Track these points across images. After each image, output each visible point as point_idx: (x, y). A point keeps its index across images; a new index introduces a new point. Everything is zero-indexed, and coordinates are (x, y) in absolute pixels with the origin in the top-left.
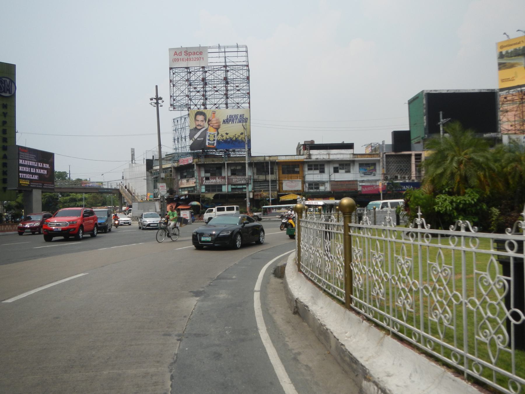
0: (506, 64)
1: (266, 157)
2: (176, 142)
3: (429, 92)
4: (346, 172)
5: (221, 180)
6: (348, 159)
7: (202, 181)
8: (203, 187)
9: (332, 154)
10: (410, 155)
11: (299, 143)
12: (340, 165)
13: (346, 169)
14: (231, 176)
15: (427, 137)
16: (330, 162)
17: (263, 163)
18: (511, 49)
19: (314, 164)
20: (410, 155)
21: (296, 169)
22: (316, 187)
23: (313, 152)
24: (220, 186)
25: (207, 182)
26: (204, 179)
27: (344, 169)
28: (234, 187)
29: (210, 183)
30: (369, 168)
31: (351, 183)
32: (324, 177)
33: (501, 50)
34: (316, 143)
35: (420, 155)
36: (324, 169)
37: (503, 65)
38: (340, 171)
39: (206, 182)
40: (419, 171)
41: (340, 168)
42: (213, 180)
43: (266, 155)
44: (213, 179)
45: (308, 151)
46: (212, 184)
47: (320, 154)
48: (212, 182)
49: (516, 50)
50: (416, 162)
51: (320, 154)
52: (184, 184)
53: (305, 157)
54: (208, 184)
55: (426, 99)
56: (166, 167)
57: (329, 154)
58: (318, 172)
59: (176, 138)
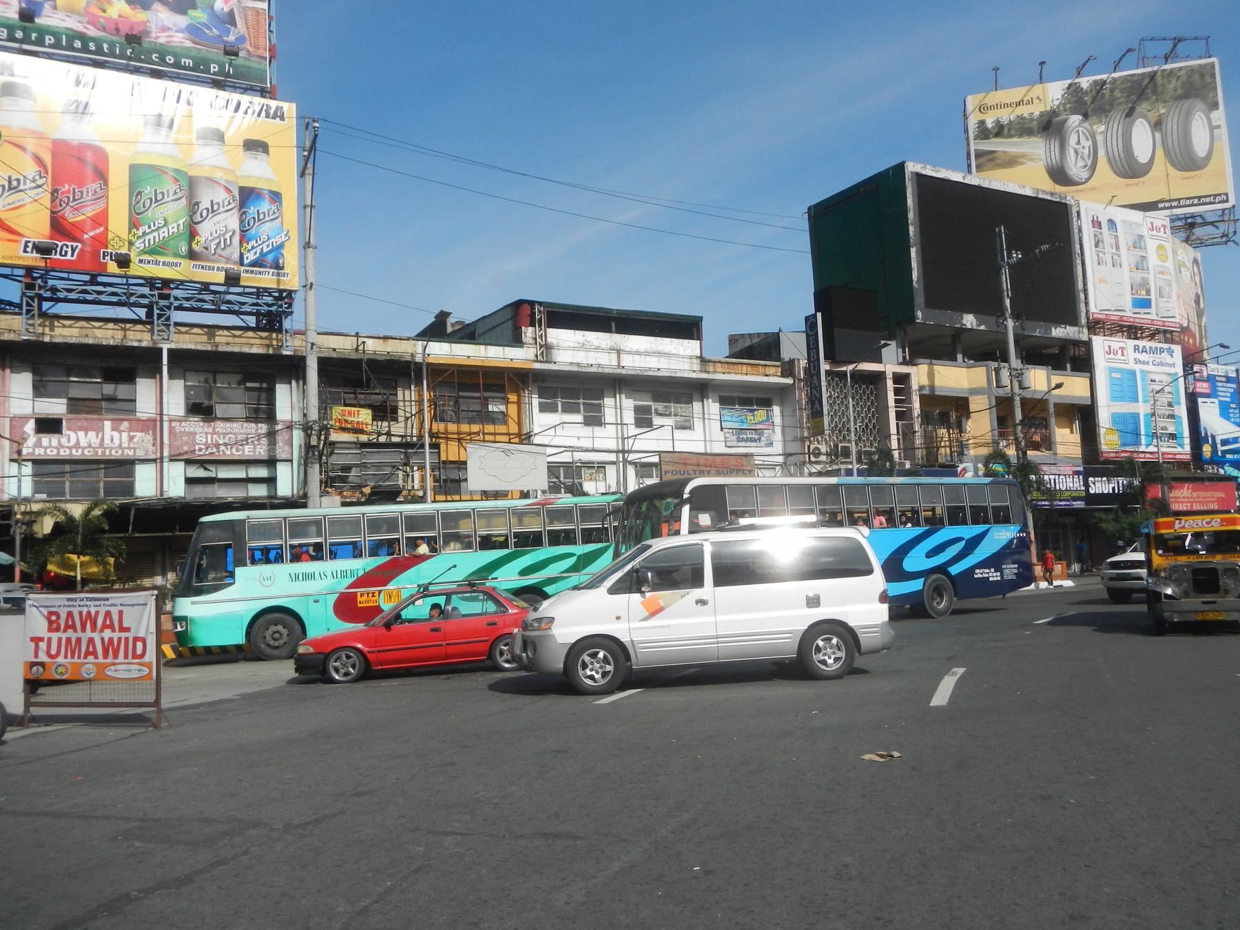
0: (996, 155)
5: (131, 439)
9: (630, 353)
11: (450, 314)
13: (675, 415)
18: (1006, 116)
20: (879, 377)
24: (125, 466)
26: (30, 426)
27: (670, 415)
28: (200, 473)
30: (754, 416)
33: (981, 117)
36: (599, 408)
37: (989, 157)
38: (657, 421)
39: (38, 444)
40: (907, 434)
41: (656, 410)
42: (81, 434)
44: (86, 430)
45: (543, 332)
47: (583, 347)
48: (77, 446)
49: (1021, 118)
50: (896, 401)
57: (619, 352)
58: (579, 418)
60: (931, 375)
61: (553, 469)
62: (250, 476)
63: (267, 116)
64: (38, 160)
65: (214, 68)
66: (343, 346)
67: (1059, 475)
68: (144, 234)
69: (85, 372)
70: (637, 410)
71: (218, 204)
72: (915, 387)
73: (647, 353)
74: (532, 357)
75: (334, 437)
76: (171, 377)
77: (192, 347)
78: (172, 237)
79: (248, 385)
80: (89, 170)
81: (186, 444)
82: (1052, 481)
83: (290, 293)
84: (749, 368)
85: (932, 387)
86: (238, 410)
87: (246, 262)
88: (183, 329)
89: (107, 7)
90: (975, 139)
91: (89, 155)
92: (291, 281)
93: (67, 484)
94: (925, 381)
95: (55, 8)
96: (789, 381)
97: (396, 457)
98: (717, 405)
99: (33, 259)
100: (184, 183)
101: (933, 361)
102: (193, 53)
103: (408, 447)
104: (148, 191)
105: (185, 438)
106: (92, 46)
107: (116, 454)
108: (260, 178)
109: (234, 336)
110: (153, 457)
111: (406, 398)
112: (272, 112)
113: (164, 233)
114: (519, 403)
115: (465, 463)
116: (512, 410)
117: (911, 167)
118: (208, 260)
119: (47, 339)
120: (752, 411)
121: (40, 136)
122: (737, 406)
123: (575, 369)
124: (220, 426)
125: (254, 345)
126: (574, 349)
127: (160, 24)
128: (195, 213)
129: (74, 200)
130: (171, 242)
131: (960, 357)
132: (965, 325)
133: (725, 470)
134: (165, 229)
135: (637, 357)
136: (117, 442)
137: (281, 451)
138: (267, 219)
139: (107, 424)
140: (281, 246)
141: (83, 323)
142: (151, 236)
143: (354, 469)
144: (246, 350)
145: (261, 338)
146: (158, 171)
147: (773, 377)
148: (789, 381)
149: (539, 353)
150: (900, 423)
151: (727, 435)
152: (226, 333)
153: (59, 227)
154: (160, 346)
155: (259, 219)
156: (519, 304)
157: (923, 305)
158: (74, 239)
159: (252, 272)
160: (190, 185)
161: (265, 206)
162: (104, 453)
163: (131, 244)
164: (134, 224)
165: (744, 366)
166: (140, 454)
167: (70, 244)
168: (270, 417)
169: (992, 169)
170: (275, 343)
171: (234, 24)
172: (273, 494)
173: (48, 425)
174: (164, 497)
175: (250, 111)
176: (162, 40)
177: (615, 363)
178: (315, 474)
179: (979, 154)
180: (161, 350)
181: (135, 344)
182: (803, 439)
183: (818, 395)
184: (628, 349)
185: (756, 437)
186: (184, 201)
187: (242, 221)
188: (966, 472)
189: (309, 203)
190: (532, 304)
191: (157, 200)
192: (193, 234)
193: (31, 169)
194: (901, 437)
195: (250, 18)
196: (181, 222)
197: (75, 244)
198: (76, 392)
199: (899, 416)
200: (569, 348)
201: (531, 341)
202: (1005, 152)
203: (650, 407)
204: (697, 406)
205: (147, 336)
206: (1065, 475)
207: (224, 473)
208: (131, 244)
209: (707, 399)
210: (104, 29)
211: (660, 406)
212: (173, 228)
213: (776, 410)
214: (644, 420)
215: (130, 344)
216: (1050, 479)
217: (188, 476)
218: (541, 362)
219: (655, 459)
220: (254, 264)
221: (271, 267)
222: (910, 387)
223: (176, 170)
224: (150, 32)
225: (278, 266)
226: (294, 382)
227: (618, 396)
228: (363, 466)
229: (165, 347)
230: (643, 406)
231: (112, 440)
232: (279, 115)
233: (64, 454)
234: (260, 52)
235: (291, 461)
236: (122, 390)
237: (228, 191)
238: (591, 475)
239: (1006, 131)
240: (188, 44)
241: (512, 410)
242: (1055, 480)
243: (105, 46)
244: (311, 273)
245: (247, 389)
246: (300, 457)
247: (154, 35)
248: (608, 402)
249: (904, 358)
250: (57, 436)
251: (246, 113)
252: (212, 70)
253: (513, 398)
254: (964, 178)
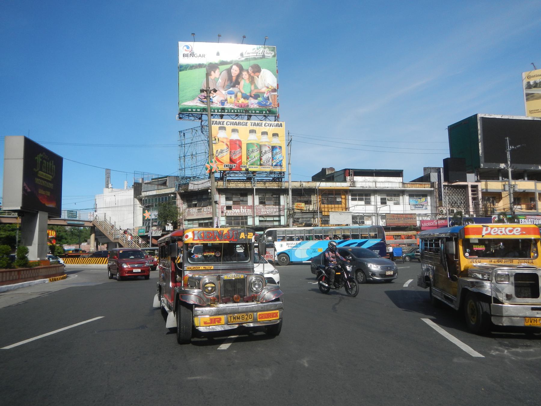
0: (534, 95)
2: (182, 160)
3: (483, 116)
4: (395, 204)
5: (247, 211)
8: (224, 219)
9: (379, 182)
14: (259, 205)
15: (483, 166)
16: (376, 192)
17: (301, 189)
19: (359, 193)
20: (466, 187)
22: (361, 221)
23: (356, 178)
24: (246, 217)
25: (228, 212)
26: (225, 207)
27: (392, 200)
28: (262, 219)
31: (409, 216)
32: (370, 209)
33: (528, 80)
35: (476, 187)
36: (370, 199)
37: (532, 95)
40: (476, 205)
41: (388, 199)
42: (236, 210)
44: (237, 209)
47: (365, 181)
50: (472, 194)
51: (365, 181)
52: (193, 215)
55: (480, 124)
56: (164, 193)
58: (363, 203)
59: (182, 155)
60: (486, 185)
61: (354, 218)
62: (274, 220)
63: (278, 126)
64: (227, 145)
65: (264, 112)
66: (297, 185)
67: (535, 219)
68: (250, 160)
69: (236, 194)
70: (381, 199)
71: (267, 151)
72: (480, 189)
73: (384, 182)
74: (349, 185)
75: (296, 211)
76: (256, 195)
77: (261, 187)
78: (256, 160)
79: (274, 196)
80: (238, 146)
81: (259, 212)
82: (532, 221)
83: (284, 172)
84: (419, 185)
85: (487, 189)
86: (272, 203)
87: (273, 165)
88: (258, 183)
89: (239, 100)
90: (526, 89)
91: (238, 142)
92: (284, 169)
93: (233, 222)
94: (484, 187)
95: (227, 103)
96: (432, 189)
97: (311, 216)
98: (408, 197)
99: (227, 169)
100: (259, 147)
101: (487, 180)
102: (259, 109)
103: (314, 212)
104: (251, 150)
105: (259, 210)
106: (236, 111)
107: (244, 215)
108: (276, 143)
109: (270, 184)
110: (252, 215)
111: (314, 198)
112: (279, 125)
113: (254, 159)
114: (345, 199)
115: (329, 215)
116: (343, 201)
117: (479, 116)
118: (264, 166)
119: (229, 187)
120: (420, 198)
121: (227, 138)
122: (415, 197)
123: (362, 188)
124: (267, 206)
125: (274, 186)
126: (362, 182)
127: (251, 103)
128: (261, 154)
129: (235, 154)
130: (256, 162)
131: (500, 178)
132: (501, 167)
133: (406, 218)
134: (254, 159)
135: (382, 184)
136: (244, 211)
137: (282, 213)
138: (278, 153)
139: (241, 207)
140: (282, 160)
141: (236, 183)
142: (251, 161)
143: (300, 219)
144: (273, 188)
145: (277, 184)
146: (252, 144)
147: (427, 187)
148: (432, 189)
149: (351, 184)
150: (474, 201)
151: (411, 206)
152: (268, 183)
153: (232, 161)
154: (253, 188)
155: (276, 154)
156: (345, 170)
157: (483, 162)
158: (235, 163)
159: (275, 168)
160: (260, 147)
161: (278, 150)
162: (241, 214)
163: (247, 163)
164: (248, 158)
165: (417, 185)
166: (249, 214)
167: (234, 164)
168: (279, 204)
169: (533, 100)
170: (280, 185)
171: (269, 100)
172: (280, 224)
173: (229, 208)
174: (255, 225)
175: (274, 126)
176: (252, 107)
177: (374, 186)
178: (291, 220)
179: (527, 95)
180: (254, 189)
181: (248, 188)
182: (437, 207)
183: (441, 194)
184: (379, 181)
185: (421, 207)
186: (259, 151)
187: (272, 155)
188: (495, 218)
189: (290, 153)
190: (349, 169)
191: (252, 152)
192: (261, 159)
193: (225, 147)
194: (474, 206)
195: (273, 97)
196: (258, 157)
197: (235, 164)
198: (235, 199)
199: (474, 199)
201: (349, 180)
202: (538, 93)
203: (386, 198)
204: (401, 197)
205: (250, 185)
206: (538, 219)
207: (268, 219)
208: (247, 163)
209: (405, 195)
210: (238, 106)
211: (389, 198)
212: (256, 158)
213: (429, 198)
214: (383, 202)
215: (247, 188)
216: (531, 221)
217: (260, 220)
218: (352, 187)
219: (385, 214)
220: (276, 165)
221: (279, 166)
222: (478, 190)
223: (257, 144)
224: (249, 105)
225: (281, 166)
226: (285, 195)
227: (375, 195)
228: (303, 218)
229: (255, 188)
230: (383, 198)
231: (243, 211)
232: (281, 125)
233: (232, 215)
234: (275, 106)
235: (284, 216)
236: (245, 198)
237: (269, 147)
238: (367, 219)
239: (538, 85)
240: (258, 107)
241: (343, 201)
242: (533, 221)
243: (239, 111)
244: (290, 171)
245: (273, 197)
246: (286, 215)
247: (250, 106)
248: (372, 198)
249: (478, 179)
250: (231, 210)
251: (273, 126)
252: (264, 113)
253: (343, 197)
254: (502, 117)
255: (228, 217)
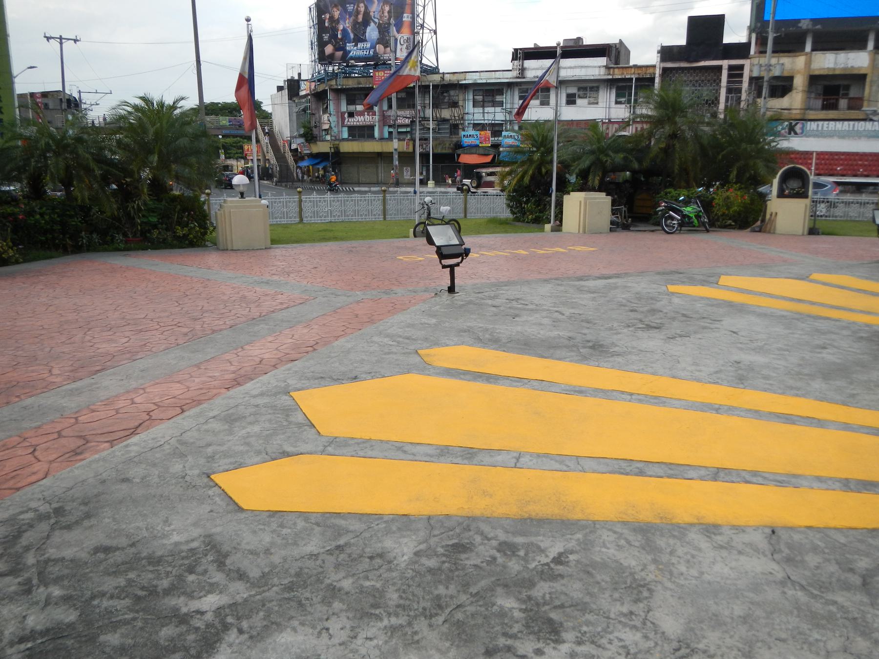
1: (446, 76)
6: (592, 78)
7: (343, 119)
8: (345, 130)
9: (565, 68)
10: (720, 68)
12: (579, 89)
20: (720, 68)
21: (498, 98)
26: (346, 115)
27: (586, 98)
29: (355, 123)
34: (587, 42)
36: (549, 97)
39: (348, 121)
43: (445, 72)
46: (358, 124)
50: (728, 82)
53: (515, 73)
54: (352, 124)
73: (575, 67)
135: (569, 70)
150: (730, 95)
200: (534, 69)
255: (351, 129)
